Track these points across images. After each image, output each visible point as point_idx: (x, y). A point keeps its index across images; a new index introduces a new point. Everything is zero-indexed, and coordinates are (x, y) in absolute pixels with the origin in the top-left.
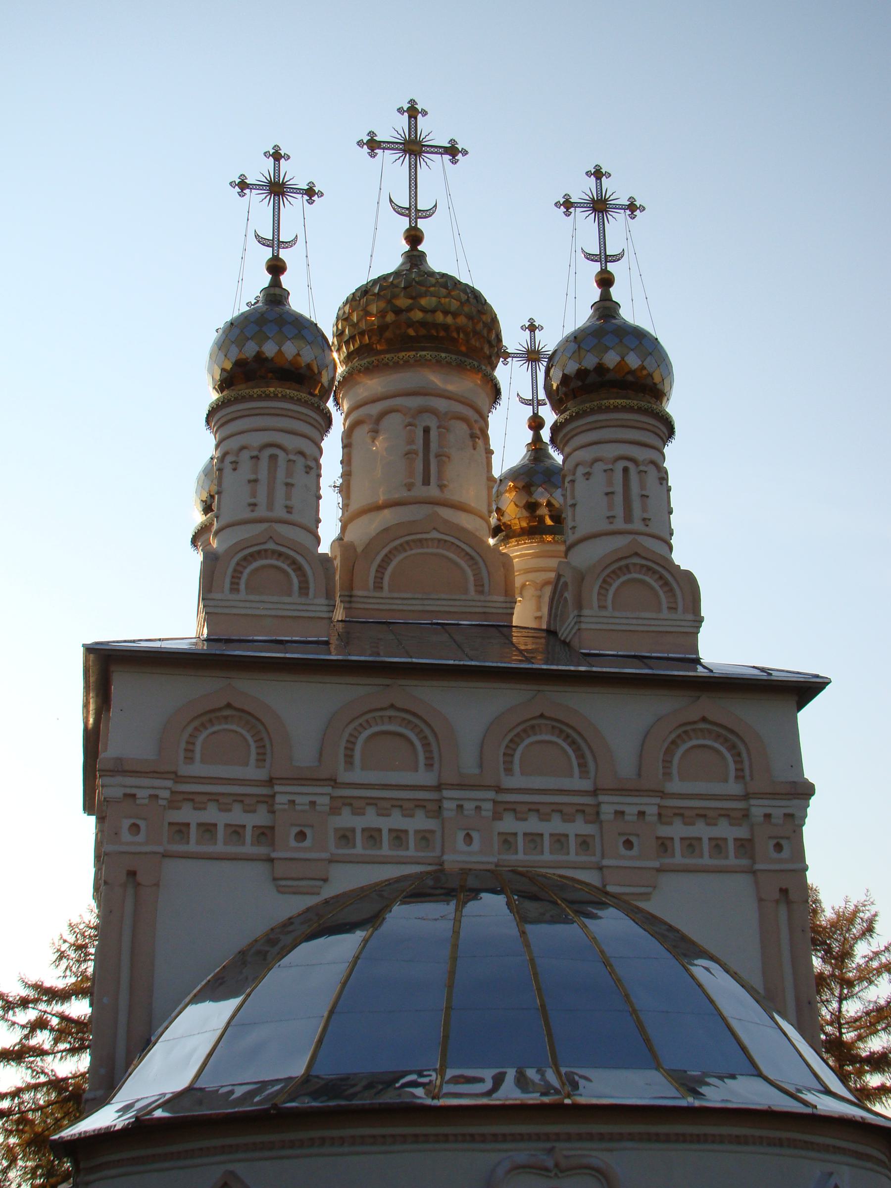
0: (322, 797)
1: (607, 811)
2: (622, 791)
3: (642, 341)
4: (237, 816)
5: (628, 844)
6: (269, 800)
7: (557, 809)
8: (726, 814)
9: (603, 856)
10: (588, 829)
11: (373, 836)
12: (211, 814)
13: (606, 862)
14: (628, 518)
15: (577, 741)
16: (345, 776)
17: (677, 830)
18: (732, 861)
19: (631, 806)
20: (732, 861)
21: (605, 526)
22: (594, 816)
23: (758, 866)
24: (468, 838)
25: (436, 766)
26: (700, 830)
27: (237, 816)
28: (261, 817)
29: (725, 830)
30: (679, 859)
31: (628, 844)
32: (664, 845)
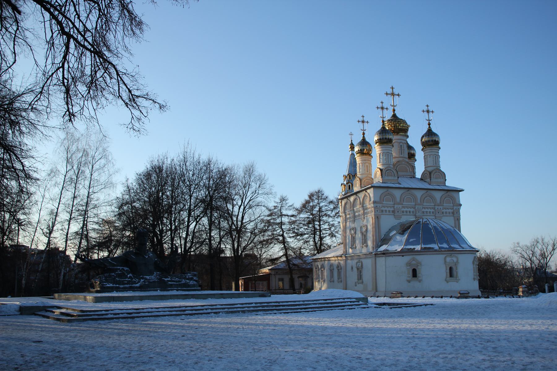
1: (436, 208)
2: (438, 206)
3: (435, 135)
4: (389, 209)
6: (394, 207)
7: (430, 208)
8: (451, 209)
11: (406, 212)
12: (386, 209)
15: (432, 197)
17: (444, 211)
19: (439, 207)
21: (432, 165)
22: (434, 209)
26: (447, 211)
27: (389, 209)
28: (392, 209)
29: (451, 211)
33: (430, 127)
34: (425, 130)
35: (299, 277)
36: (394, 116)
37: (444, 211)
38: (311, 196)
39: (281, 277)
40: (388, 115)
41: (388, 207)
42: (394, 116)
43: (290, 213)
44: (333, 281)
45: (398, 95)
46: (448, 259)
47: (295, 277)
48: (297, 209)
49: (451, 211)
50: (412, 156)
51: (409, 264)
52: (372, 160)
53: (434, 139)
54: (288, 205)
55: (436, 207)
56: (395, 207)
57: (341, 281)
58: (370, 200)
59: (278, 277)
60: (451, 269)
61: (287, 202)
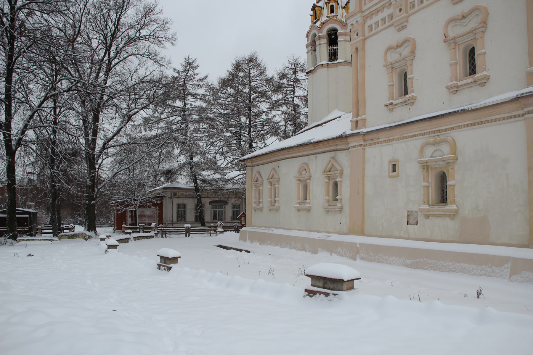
35: (210, 203)
38: (238, 67)
39: (181, 201)
43: (201, 91)
44: (309, 210)
47: (206, 202)
48: (211, 88)
54: (197, 77)
57: (341, 209)
59: (176, 201)
61: (196, 71)
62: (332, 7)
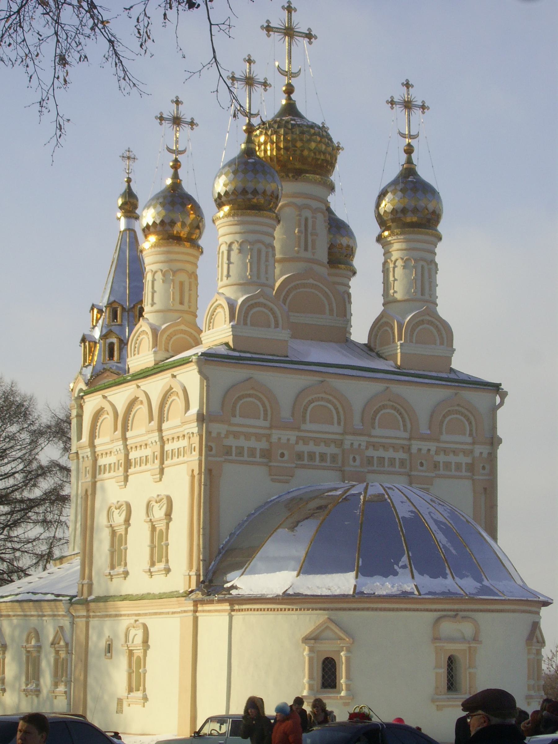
0: (292, 436)
5: (422, 464)
6: (268, 436)
9: (411, 470)
10: (404, 456)
11: (312, 456)
13: (413, 473)
14: (423, 294)
16: (303, 427)
17: (441, 458)
18: (464, 473)
19: (425, 446)
20: (464, 473)
23: (476, 477)
24: (354, 459)
25: (342, 423)
26: (452, 458)
27: (253, 443)
28: (263, 445)
29: (463, 460)
30: (442, 472)
31: (422, 464)
32: (436, 466)
33: (409, 161)
34: (394, 170)
36: (290, 109)
37: (441, 458)
40: (269, 105)
41: (247, 436)
42: (290, 109)
45: (309, 36)
46: (448, 627)
49: (463, 460)
50: (340, 257)
51: (312, 639)
52: (202, 261)
53: (422, 203)
55: (416, 445)
56: (274, 439)
58: (187, 408)
60: (451, 662)
62: (111, 345)
